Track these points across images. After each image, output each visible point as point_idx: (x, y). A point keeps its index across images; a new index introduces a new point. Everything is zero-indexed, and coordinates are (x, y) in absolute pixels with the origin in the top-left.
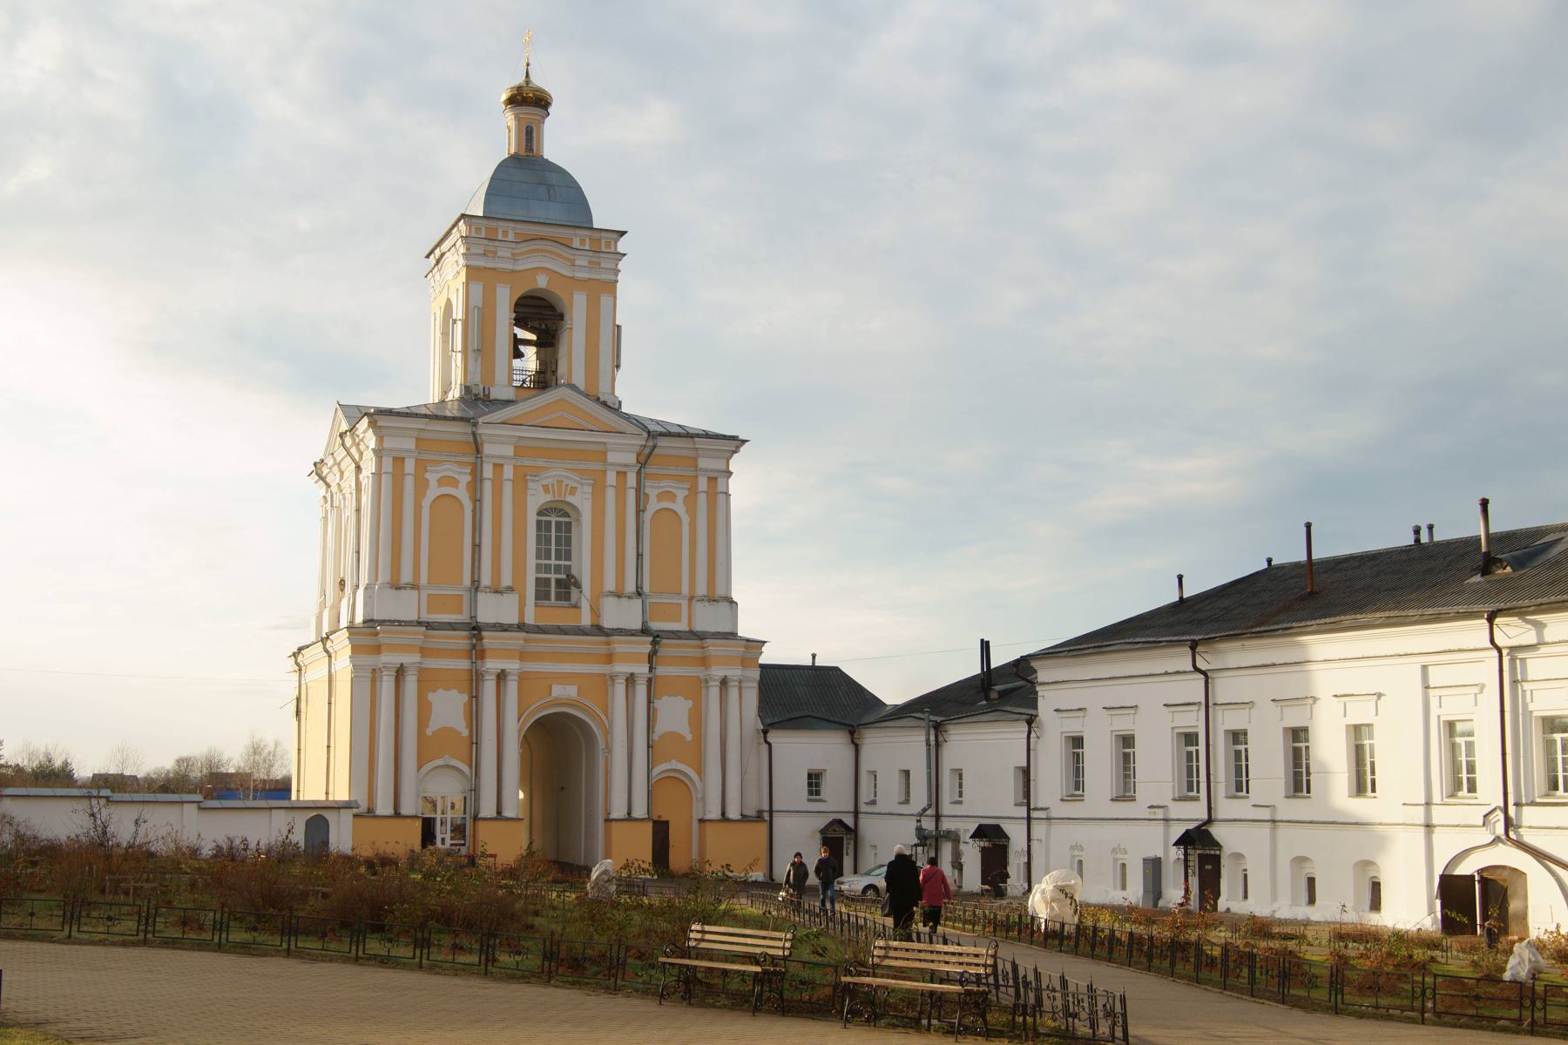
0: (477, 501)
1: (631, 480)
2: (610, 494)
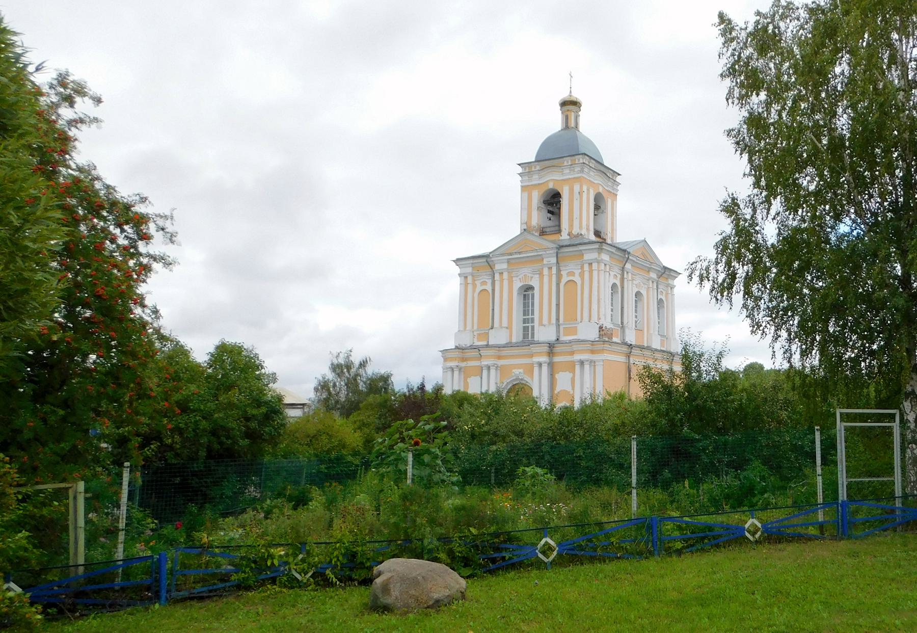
0: (493, 290)
1: (554, 270)
2: (546, 279)
